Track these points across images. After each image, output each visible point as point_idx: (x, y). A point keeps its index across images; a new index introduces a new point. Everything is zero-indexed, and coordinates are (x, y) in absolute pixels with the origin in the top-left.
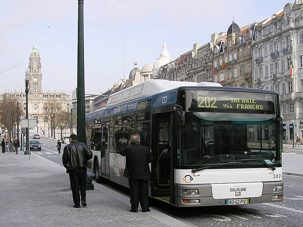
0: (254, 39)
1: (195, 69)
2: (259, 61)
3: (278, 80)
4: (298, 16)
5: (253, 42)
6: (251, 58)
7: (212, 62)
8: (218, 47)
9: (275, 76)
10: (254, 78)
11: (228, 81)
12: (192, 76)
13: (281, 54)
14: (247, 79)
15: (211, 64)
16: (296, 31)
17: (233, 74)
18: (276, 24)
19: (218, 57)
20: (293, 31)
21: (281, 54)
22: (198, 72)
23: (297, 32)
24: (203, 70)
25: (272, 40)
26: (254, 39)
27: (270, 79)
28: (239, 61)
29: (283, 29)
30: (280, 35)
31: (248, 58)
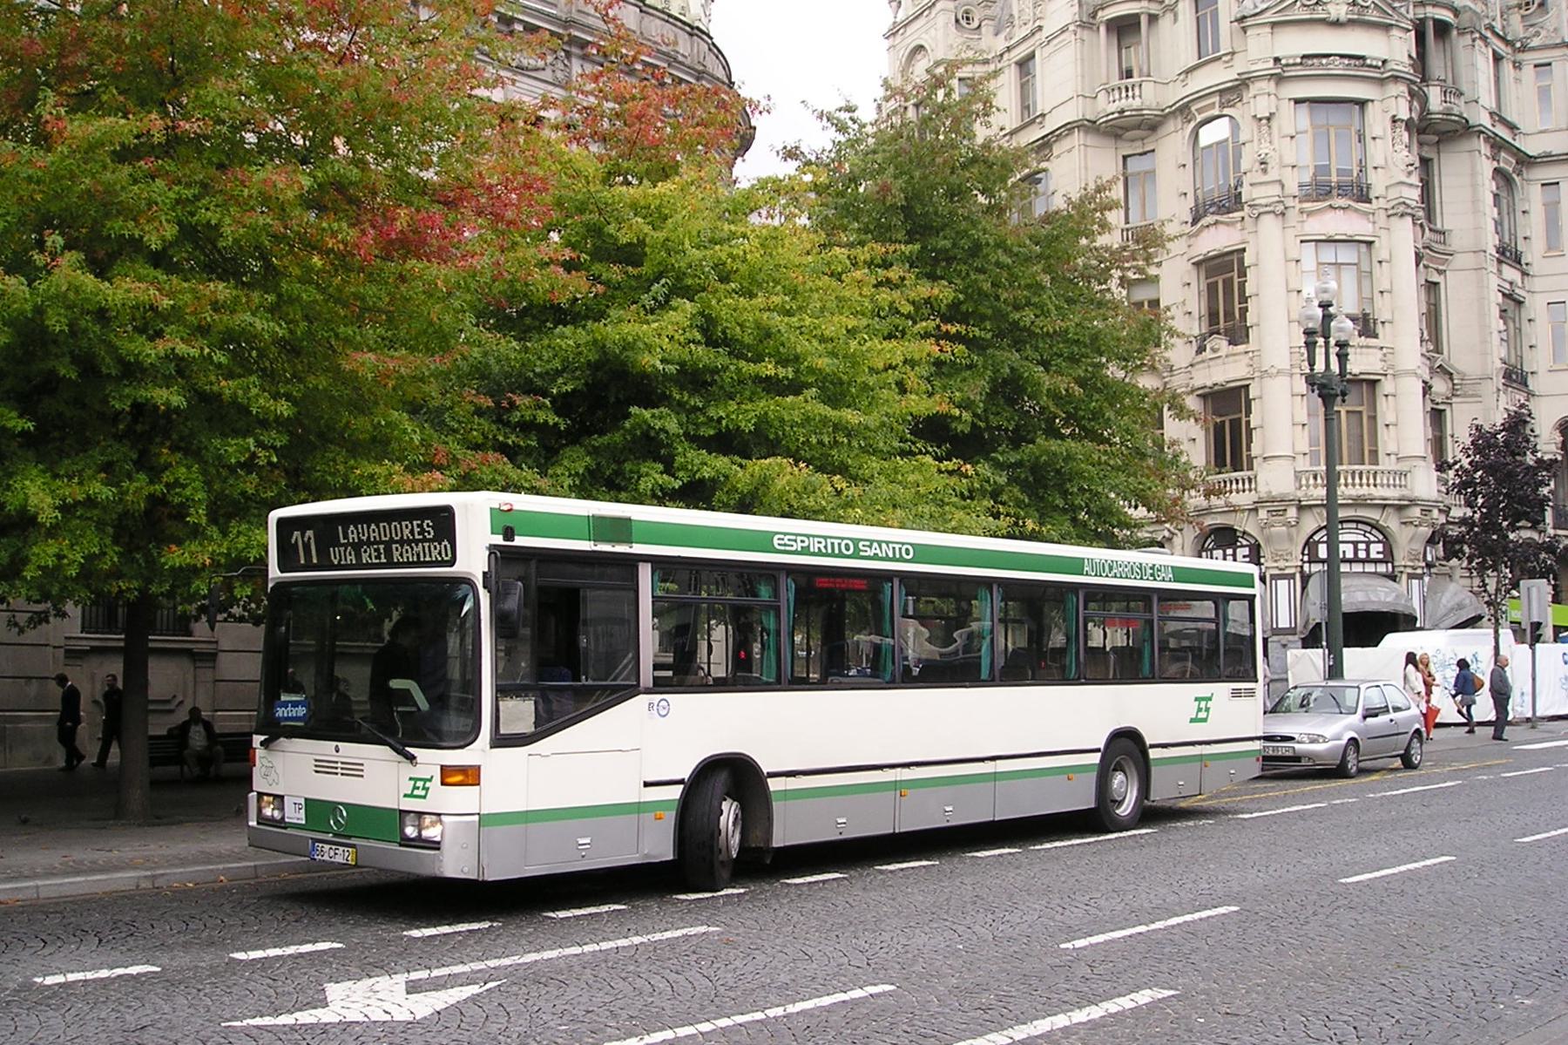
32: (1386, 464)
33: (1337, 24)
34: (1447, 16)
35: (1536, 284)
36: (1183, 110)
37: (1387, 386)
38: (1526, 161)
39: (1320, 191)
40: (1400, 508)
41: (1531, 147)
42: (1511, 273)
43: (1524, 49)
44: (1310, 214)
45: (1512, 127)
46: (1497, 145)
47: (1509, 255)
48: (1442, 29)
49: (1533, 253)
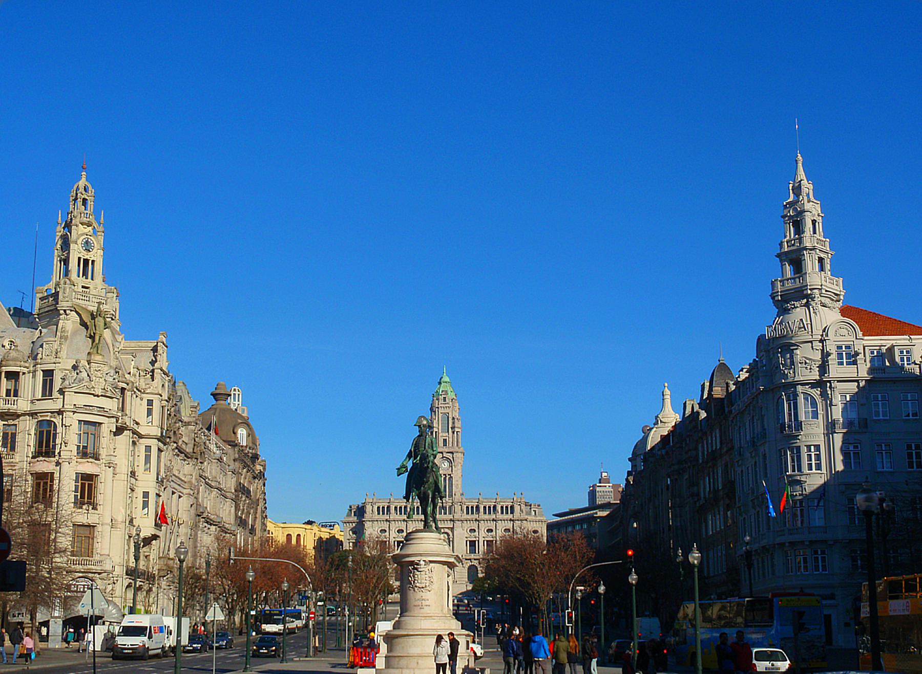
7: (696, 449)
32: (97, 558)
33: (98, 396)
34: (124, 385)
35: (139, 483)
36: (33, 414)
37: (99, 528)
38: (141, 436)
39: (84, 453)
40: (99, 574)
41: (142, 430)
42: (133, 480)
43: (144, 393)
44: (80, 463)
45: (137, 424)
46: (135, 432)
47: (133, 474)
48: (123, 389)
49: (140, 472)
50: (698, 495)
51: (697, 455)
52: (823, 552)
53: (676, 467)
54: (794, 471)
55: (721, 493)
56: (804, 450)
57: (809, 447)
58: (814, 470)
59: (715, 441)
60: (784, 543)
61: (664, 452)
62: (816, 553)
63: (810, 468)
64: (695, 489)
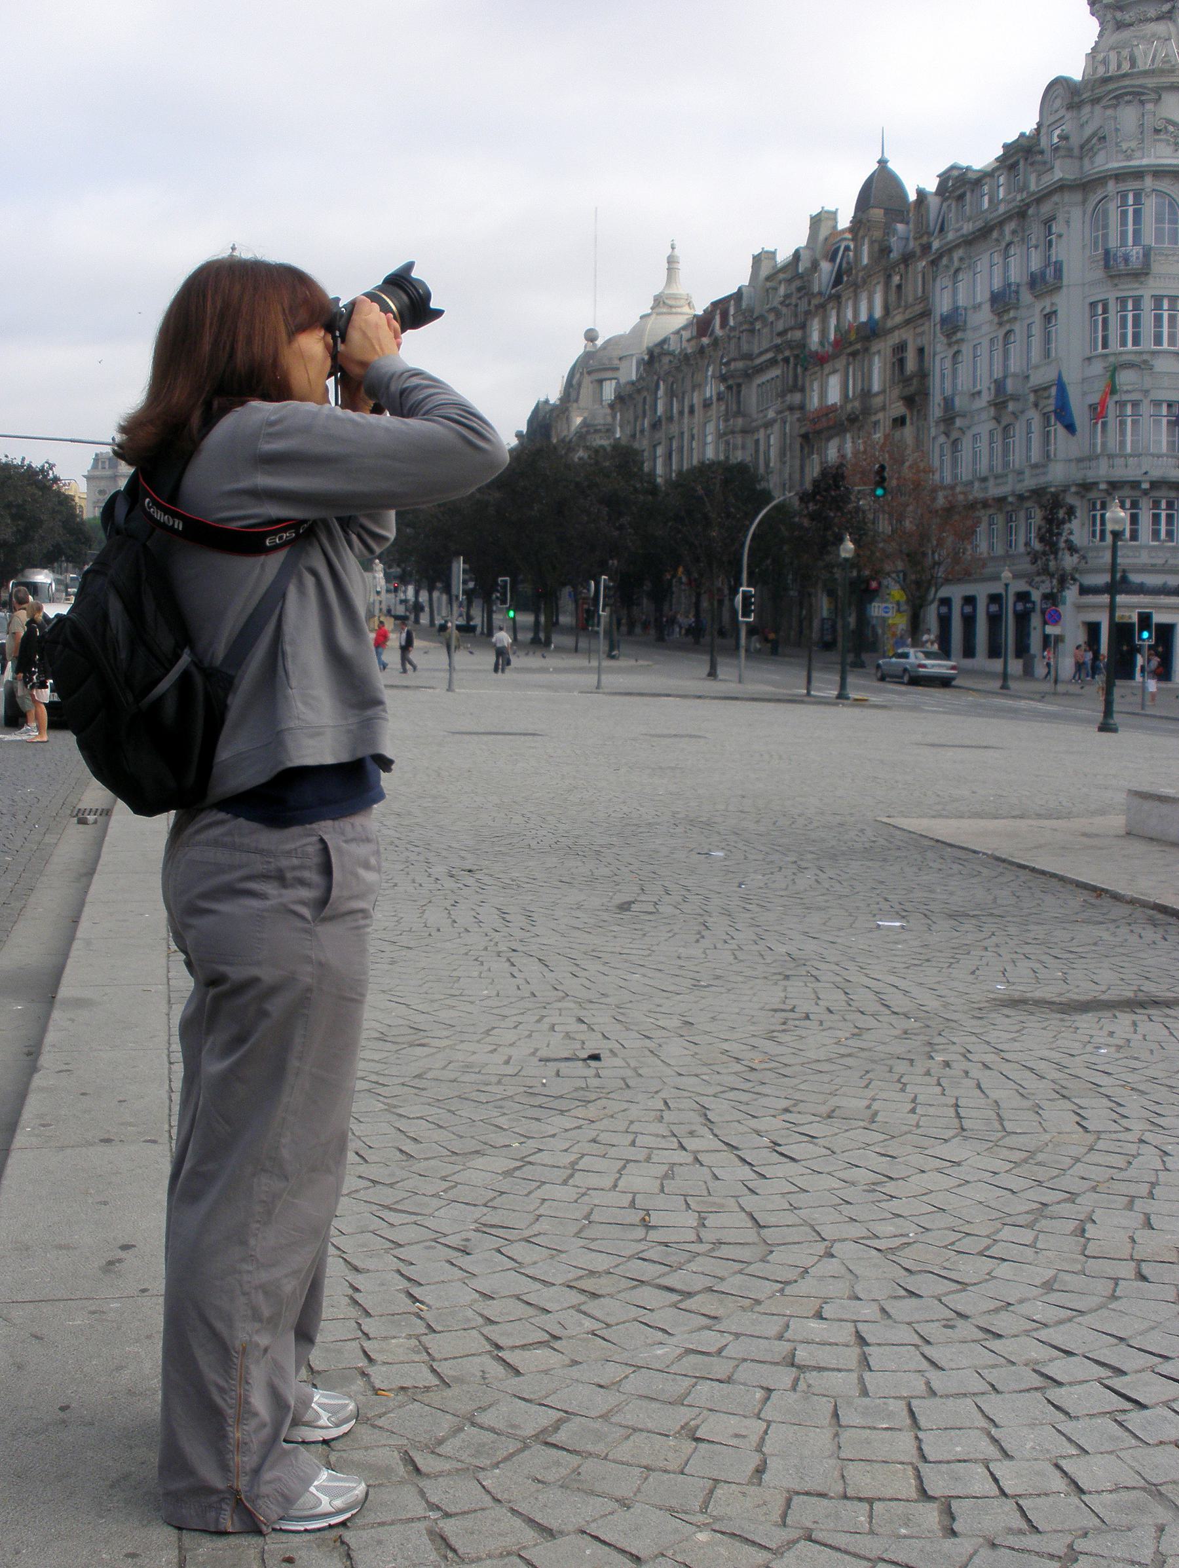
0: (942, 230)
1: (749, 357)
2: (953, 325)
3: (1011, 406)
4: (1088, 131)
5: (936, 245)
6: (926, 314)
7: (803, 326)
8: (825, 266)
9: (999, 385)
10: (936, 399)
11: (849, 407)
12: (739, 385)
13: (1026, 297)
14: (909, 401)
15: (798, 334)
16: (1078, 197)
17: (867, 377)
18: (1013, 167)
19: (822, 307)
20: (1068, 197)
21: (1026, 297)
22: (760, 370)
23: (1084, 202)
24: (773, 362)
25: (995, 234)
26: (942, 230)
27: (986, 397)
28: (890, 324)
29: (1033, 187)
30: (1021, 214)
31: (918, 309)
50: (802, 407)
51: (805, 337)
52: (1170, 505)
53: (740, 365)
54: (1124, 343)
55: (877, 401)
56: (1147, 304)
57: (1158, 300)
58: (1165, 346)
59: (868, 306)
60: (1096, 484)
61: (705, 340)
62: (1156, 504)
63: (1158, 340)
64: (797, 398)
